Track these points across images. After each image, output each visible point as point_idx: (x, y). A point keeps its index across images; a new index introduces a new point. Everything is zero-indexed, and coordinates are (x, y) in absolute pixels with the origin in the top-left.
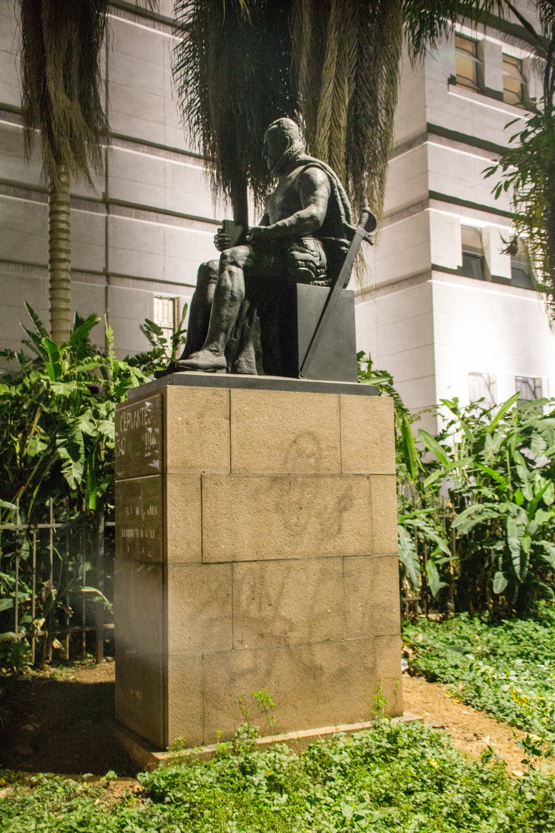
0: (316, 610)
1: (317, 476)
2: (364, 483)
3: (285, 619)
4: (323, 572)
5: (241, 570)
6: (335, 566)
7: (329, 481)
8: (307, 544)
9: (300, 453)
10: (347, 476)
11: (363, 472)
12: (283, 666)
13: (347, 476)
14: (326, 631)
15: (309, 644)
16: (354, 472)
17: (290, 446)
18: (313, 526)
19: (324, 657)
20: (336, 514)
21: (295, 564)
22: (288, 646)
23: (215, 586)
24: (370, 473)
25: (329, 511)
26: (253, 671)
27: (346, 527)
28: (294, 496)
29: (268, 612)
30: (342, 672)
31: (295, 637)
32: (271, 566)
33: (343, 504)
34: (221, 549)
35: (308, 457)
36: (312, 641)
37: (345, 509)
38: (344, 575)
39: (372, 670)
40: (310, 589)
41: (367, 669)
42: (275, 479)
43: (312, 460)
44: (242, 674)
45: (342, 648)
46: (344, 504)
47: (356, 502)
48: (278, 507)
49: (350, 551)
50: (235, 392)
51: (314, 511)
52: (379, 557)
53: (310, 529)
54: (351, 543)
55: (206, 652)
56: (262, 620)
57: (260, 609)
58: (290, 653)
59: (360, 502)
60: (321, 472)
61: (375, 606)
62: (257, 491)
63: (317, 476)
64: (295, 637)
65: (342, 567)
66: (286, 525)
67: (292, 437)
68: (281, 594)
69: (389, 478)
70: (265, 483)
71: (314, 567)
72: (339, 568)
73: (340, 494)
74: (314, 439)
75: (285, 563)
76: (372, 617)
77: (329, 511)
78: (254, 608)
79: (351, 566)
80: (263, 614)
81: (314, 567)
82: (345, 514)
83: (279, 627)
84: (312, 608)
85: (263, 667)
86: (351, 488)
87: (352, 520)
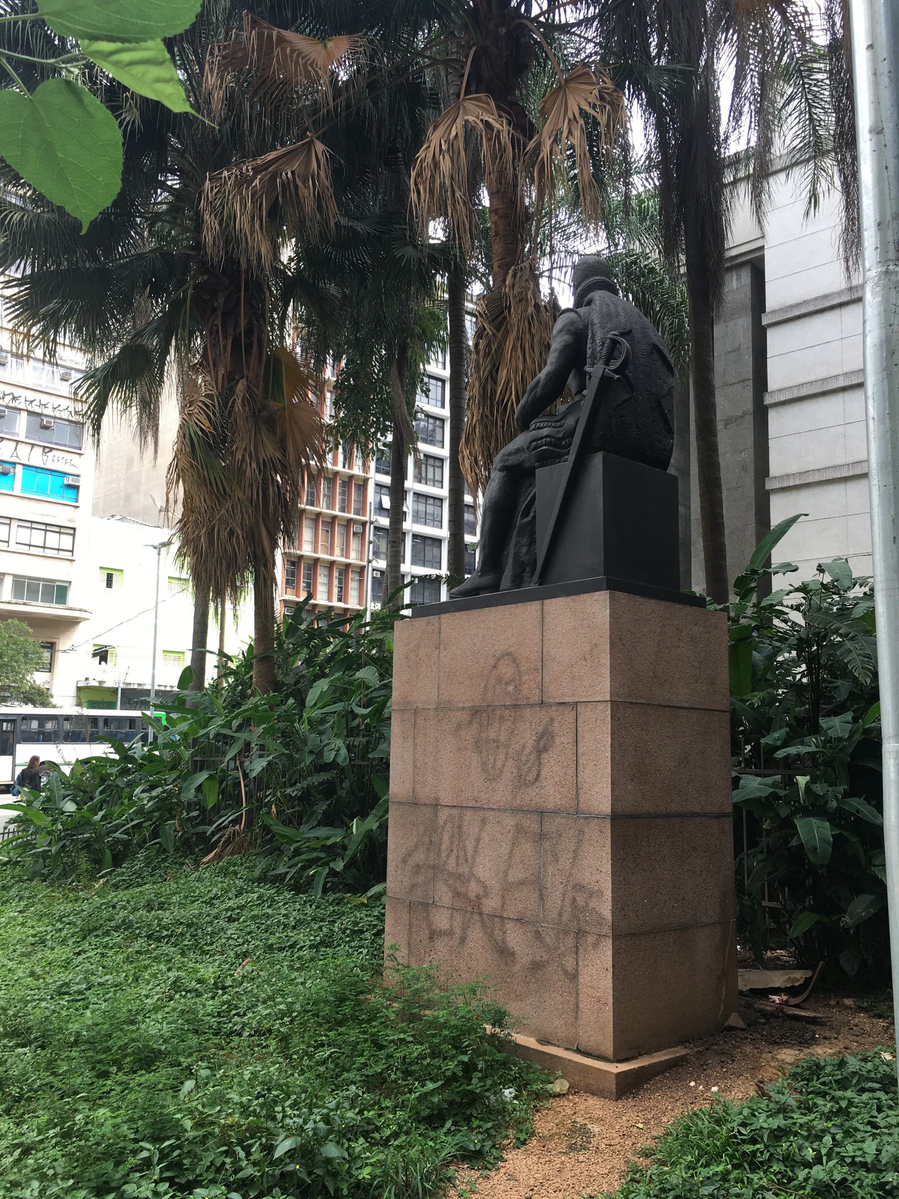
0: (511, 879)
2: (570, 716)
3: (479, 881)
4: (519, 829)
5: (444, 814)
7: (527, 713)
8: (501, 792)
9: (499, 680)
10: (550, 705)
11: (566, 700)
13: (550, 705)
14: (520, 906)
15: (502, 918)
16: (557, 700)
17: (490, 672)
18: (509, 772)
19: (515, 938)
21: (491, 816)
22: (481, 914)
24: (577, 700)
25: (527, 751)
27: (543, 774)
29: (464, 869)
30: (536, 966)
32: (469, 814)
33: (542, 743)
35: (507, 684)
37: (545, 749)
38: (542, 836)
39: (574, 977)
40: (504, 849)
41: (566, 972)
42: (475, 712)
43: (510, 688)
46: (544, 743)
48: (478, 745)
49: (551, 806)
52: (586, 818)
54: (551, 792)
56: (459, 877)
57: (457, 865)
59: (563, 739)
60: (521, 702)
61: (579, 887)
62: (459, 727)
63: (515, 706)
65: (540, 826)
67: (492, 662)
69: (601, 707)
70: (465, 717)
71: (509, 822)
72: (535, 827)
73: (541, 729)
74: (514, 660)
75: (481, 813)
77: (527, 751)
78: (452, 862)
79: (553, 825)
80: (459, 871)
81: (509, 822)
82: (545, 756)
84: (506, 873)
85: (458, 932)
86: (552, 720)
87: (554, 766)
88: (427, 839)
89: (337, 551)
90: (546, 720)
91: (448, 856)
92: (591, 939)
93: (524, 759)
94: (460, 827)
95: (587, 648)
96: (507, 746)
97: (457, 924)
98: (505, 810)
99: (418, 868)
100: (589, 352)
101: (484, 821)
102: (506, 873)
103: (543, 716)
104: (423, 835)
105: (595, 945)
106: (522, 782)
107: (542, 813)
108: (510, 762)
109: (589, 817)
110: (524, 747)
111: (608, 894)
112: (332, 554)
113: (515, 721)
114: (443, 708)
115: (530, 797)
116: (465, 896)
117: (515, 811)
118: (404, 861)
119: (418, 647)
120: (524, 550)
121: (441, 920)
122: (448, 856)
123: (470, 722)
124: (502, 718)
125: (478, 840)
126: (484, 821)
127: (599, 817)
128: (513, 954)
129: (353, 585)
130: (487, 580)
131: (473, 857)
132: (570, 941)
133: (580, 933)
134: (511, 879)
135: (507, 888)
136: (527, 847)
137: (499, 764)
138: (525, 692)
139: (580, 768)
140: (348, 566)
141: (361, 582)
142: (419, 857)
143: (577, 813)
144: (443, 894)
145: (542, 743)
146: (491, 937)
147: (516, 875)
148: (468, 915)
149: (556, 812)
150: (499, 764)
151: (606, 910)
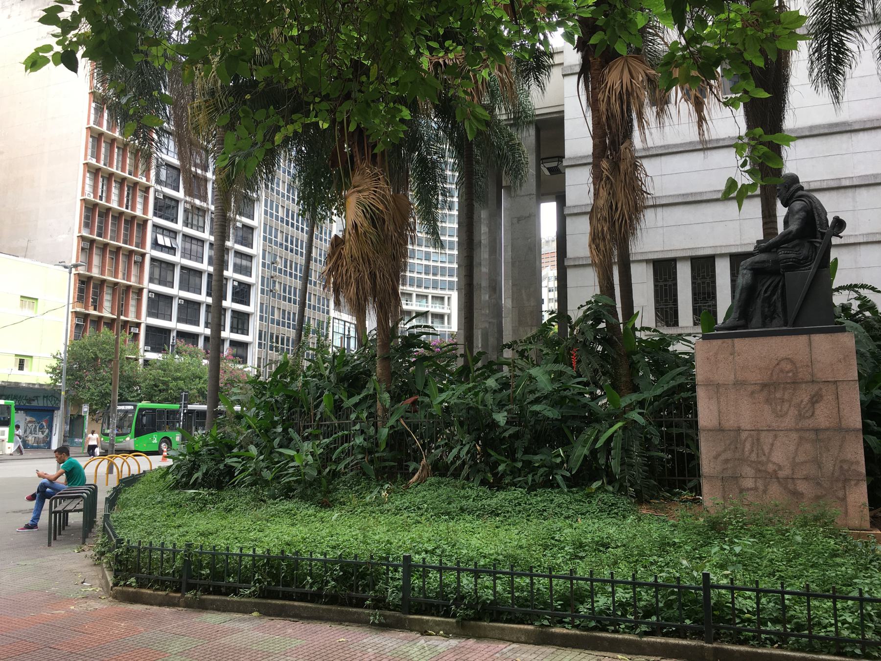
1: (793, 383)
2: (832, 387)
3: (774, 463)
4: (801, 438)
5: (744, 435)
6: (812, 436)
7: (804, 386)
9: (782, 371)
12: (775, 489)
15: (793, 478)
18: (793, 412)
20: (809, 405)
21: (781, 433)
22: (778, 478)
23: (728, 442)
26: (756, 489)
27: (817, 412)
28: (778, 395)
29: (764, 459)
31: (781, 474)
33: (815, 399)
34: (730, 422)
35: (788, 372)
36: (795, 476)
37: (817, 402)
39: (844, 499)
40: (792, 448)
41: (838, 498)
42: (764, 386)
43: (791, 374)
44: (748, 489)
45: (818, 484)
46: (816, 399)
47: (825, 398)
48: (768, 401)
49: (823, 426)
50: (736, 340)
51: (793, 403)
53: (790, 413)
55: (725, 475)
58: (779, 482)
59: (829, 397)
62: (753, 393)
63: (793, 383)
64: (781, 474)
66: (774, 411)
68: (771, 449)
70: (758, 388)
71: (794, 436)
73: (813, 393)
75: (774, 433)
76: (841, 467)
80: (760, 459)
81: (794, 436)
82: (817, 406)
83: (771, 467)
84: (794, 458)
85: (761, 488)
86: (821, 389)
88: (732, 447)
89: (120, 275)
90: (816, 389)
91: (750, 454)
92: (853, 483)
93: (802, 406)
94: (758, 440)
95: (841, 357)
96: (790, 401)
97: (760, 484)
98: (791, 430)
99: (727, 461)
100: (818, 222)
101: (776, 436)
102: (794, 458)
103: (816, 388)
104: (730, 445)
105: (856, 485)
106: (801, 417)
107: (817, 431)
108: (792, 408)
109: (848, 430)
110: (802, 401)
111: (864, 462)
112: (116, 277)
113: (794, 389)
114: (739, 384)
115: (808, 423)
116: (766, 471)
117: (797, 430)
118: (716, 457)
119: (716, 354)
120: (766, 309)
121: (749, 483)
122: (750, 454)
123: (762, 390)
124: (785, 389)
125: (772, 445)
126: (776, 436)
127: (855, 430)
128: (802, 494)
129: (132, 303)
130: (742, 322)
131: (770, 453)
132: (840, 485)
133: (846, 481)
134: (797, 460)
135: (794, 465)
136: (808, 446)
137: (785, 409)
138: (800, 375)
139: (841, 410)
140: (129, 287)
141: (139, 301)
142: (728, 455)
143: (840, 430)
144: (748, 471)
145: (815, 399)
146: (785, 488)
147: (801, 458)
148: (768, 480)
149: (827, 429)
150: (785, 409)
151: (863, 469)
